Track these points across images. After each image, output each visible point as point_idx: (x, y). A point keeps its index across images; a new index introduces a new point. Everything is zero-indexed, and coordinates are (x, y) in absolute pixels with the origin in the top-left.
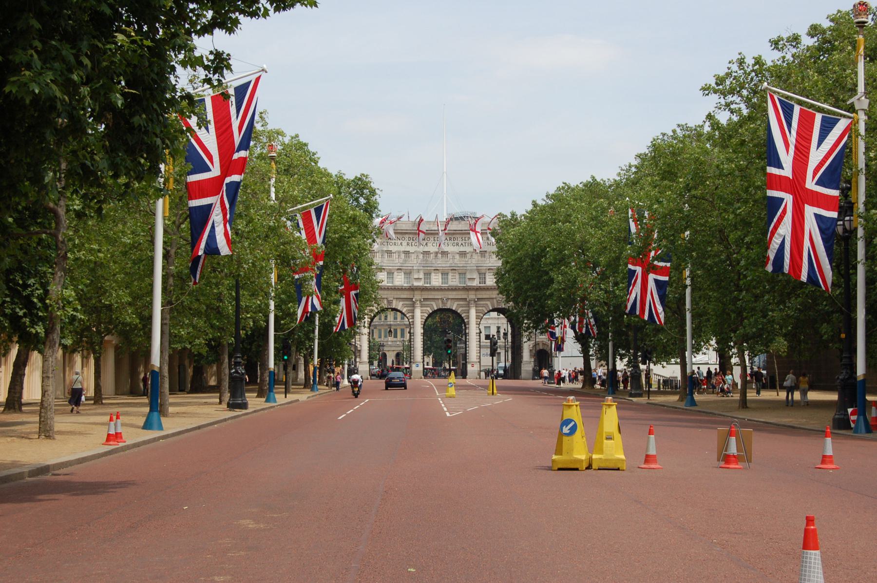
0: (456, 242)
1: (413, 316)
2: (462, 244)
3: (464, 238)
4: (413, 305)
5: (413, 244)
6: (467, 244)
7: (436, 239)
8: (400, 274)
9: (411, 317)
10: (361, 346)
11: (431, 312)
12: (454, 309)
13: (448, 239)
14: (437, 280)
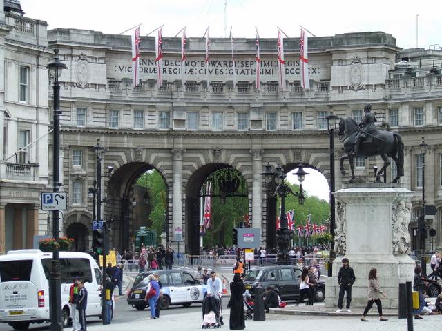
2: (243, 72)
4: (172, 160)
5: (172, 70)
6: (250, 72)
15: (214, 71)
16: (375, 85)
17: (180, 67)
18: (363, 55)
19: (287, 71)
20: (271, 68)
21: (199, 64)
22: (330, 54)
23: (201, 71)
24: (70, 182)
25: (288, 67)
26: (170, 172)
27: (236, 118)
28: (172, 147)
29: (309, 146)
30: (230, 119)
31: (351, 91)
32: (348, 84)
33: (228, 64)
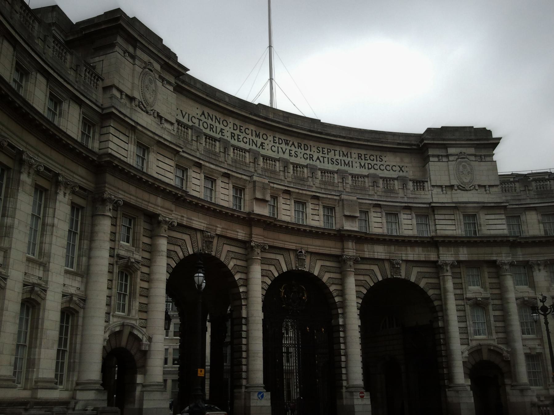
0: (308, 152)
2: (318, 158)
3: (321, 149)
4: (248, 260)
5: (241, 138)
6: (326, 160)
7: (277, 139)
8: (227, 186)
10: (150, 339)
11: (276, 275)
12: (316, 273)
13: (296, 145)
14: (288, 213)
15: (288, 151)
16: (490, 186)
17: (249, 136)
18: (472, 151)
19: (370, 166)
20: (349, 159)
21: (271, 138)
22: (427, 147)
23: (273, 148)
24: (116, 270)
25: (369, 161)
27: (321, 212)
28: (247, 239)
29: (411, 258)
30: (315, 212)
31: (459, 191)
32: (454, 182)
33: (302, 147)
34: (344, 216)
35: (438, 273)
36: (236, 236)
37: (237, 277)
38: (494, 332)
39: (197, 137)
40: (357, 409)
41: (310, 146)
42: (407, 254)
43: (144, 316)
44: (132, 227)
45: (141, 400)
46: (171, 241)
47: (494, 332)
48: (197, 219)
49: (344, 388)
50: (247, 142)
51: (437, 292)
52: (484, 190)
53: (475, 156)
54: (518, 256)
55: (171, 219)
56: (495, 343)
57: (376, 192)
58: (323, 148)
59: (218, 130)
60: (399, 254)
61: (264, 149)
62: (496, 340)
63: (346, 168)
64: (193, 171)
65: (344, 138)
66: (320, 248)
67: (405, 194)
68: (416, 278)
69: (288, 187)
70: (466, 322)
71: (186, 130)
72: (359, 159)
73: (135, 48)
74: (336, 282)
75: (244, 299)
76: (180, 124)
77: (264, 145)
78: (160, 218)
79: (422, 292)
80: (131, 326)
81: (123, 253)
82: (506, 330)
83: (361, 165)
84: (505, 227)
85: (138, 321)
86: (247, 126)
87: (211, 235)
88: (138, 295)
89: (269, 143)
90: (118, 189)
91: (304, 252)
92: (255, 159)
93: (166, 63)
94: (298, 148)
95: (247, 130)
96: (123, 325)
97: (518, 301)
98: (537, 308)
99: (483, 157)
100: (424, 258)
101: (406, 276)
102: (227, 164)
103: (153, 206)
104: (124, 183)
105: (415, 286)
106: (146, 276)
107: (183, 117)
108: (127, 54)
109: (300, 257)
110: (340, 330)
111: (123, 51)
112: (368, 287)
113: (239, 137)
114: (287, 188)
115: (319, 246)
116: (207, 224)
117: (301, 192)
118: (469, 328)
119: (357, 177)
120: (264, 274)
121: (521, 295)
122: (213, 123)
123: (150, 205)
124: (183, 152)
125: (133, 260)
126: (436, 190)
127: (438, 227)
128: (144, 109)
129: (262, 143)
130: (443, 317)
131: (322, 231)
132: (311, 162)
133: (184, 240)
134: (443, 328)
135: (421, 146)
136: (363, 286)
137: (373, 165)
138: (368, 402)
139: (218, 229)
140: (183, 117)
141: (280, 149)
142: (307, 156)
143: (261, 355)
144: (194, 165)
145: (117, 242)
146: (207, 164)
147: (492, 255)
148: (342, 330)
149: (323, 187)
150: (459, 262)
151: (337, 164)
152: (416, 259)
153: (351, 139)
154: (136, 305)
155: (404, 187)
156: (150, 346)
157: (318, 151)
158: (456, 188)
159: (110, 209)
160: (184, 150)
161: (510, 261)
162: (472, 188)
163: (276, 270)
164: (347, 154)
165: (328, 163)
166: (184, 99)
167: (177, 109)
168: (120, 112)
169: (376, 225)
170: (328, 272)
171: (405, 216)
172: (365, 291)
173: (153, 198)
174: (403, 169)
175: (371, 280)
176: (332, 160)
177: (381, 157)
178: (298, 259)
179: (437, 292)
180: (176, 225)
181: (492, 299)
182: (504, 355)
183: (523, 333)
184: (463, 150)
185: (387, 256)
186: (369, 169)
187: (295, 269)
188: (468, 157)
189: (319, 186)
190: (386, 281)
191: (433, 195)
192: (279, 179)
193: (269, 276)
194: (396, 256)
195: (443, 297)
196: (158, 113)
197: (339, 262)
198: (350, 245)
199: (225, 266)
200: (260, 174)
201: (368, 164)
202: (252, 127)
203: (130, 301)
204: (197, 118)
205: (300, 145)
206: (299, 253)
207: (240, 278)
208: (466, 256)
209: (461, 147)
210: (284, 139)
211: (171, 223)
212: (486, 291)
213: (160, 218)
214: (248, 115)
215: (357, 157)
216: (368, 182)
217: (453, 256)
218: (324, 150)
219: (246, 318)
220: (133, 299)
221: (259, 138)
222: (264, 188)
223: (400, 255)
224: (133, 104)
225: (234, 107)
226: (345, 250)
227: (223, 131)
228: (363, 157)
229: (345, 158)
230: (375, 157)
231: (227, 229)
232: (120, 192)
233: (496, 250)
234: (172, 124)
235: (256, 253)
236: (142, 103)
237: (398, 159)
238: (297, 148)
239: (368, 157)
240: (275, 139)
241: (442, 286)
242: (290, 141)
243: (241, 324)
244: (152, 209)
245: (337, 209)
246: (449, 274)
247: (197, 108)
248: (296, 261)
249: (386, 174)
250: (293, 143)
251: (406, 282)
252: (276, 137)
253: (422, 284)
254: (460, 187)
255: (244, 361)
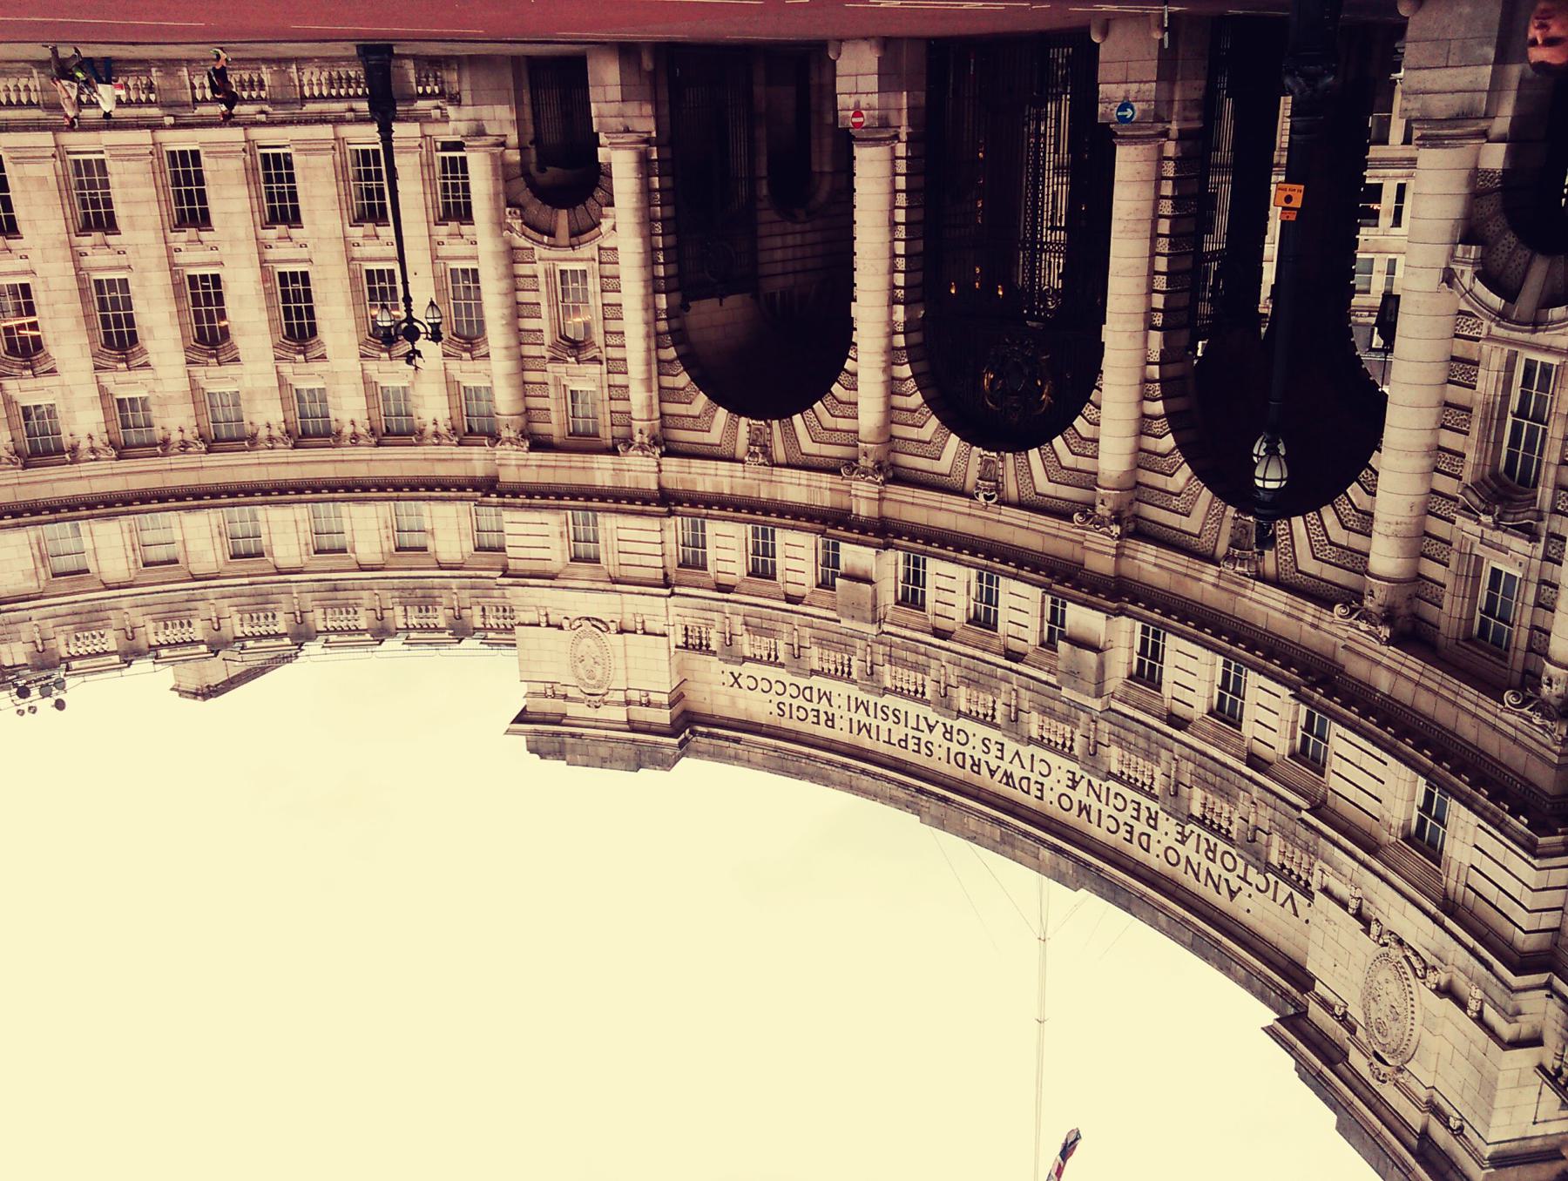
0: (955, 748)
1: (1142, 432)
2: (931, 728)
3: (924, 749)
4: (1134, 488)
5: (1130, 811)
6: (911, 722)
7: (1034, 788)
9: (1158, 426)
10: (1449, 277)
11: (1058, 442)
12: (954, 440)
14: (1015, 601)
15: (1008, 757)
16: (538, 625)
17: (1106, 811)
18: (573, 710)
19: (807, 692)
20: (855, 718)
25: (808, 706)
26: (1150, 443)
28: (1131, 543)
33: (969, 762)
34: (873, 583)
35: (663, 426)
36: (1160, 555)
37: (1169, 442)
38: (542, 279)
39: (1254, 840)
40: (872, 82)
41: (948, 762)
42: (732, 477)
43: (1460, 347)
44: (1478, 615)
45: (1496, 86)
46: (1358, 561)
47: (542, 279)
48: (1271, 612)
49: (904, 137)
50: (1116, 798)
51: (668, 381)
52: (550, 616)
53: (565, 697)
54: (482, 457)
55: (1350, 625)
56: (539, 251)
57: (796, 633)
58: (919, 752)
59: (1192, 841)
60: (750, 478)
61: (1069, 771)
62: (536, 258)
63: (863, 697)
64: (1273, 748)
65: (863, 772)
66: (938, 505)
67: (727, 621)
68: (713, 417)
69: (1011, 670)
70: (604, 305)
71: (1287, 864)
72: (833, 715)
73: (1425, 1134)
74: (905, 416)
75: (1154, 381)
76: (1302, 883)
77: (1070, 783)
78: (1385, 632)
79: (702, 381)
80: (1510, 321)
81: (1519, 545)
82: (514, 283)
83: (829, 700)
84: (508, 528)
85: (1485, 331)
86: (1112, 840)
87: (1235, 565)
88: (1478, 412)
89: (1056, 784)
90: (1515, 740)
91: (981, 496)
92: (1095, 753)
93: (1330, 1063)
94: (979, 760)
95: (1113, 828)
96: (1537, 324)
97: (483, 351)
98: (430, 336)
99: (549, 692)
100: (693, 465)
101: (737, 423)
102: (1172, 751)
103: (1405, 671)
104: (1496, 755)
105: (718, 398)
106: (1443, 467)
107: (1291, 895)
108: (1454, 1124)
109: (993, 484)
110: (903, 292)
111: (1465, 1137)
112: (828, 399)
113: (1135, 814)
114: (1014, 666)
115: (940, 509)
116: (1244, 596)
117: (978, 653)
118: (598, 289)
119: (839, 674)
120: (1091, 446)
121: (480, 365)
122: (1206, 863)
123: (1416, 677)
124: (1298, 808)
125: (1483, 518)
126: (658, 629)
127: (657, 537)
128: (1409, 953)
129: (1074, 788)
130: (657, 319)
131: (929, 548)
132: (949, 722)
133: (1315, 558)
134: (656, 291)
135: (688, 731)
136: (841, 402)
137: (801, 695)
138: (843, 101)
139: (1212, 580)
140: (1291, 895)
141: (1027, 764)
142: (959, 737)
143: (1116, 227)
144: (1270, 764)
145: (1534, 577)
146: (1230, 761)
147: (539, 463)
148: (898, 291)
149: (922, 659)
150: (613, 451)
151: (885, 709)
152: (712, 464)
153: (845, 767)
154: (1487, 383)
155: (730, 639)
156: (1452, 256)
157: (929, 745)
158: (613, 627)
159: (1550, 684)
160: (1295, 813)
161: (498, 446)
162: (577, 623)
163: (1060, 455)
164: (860, 730)
165: (906, 713)
166: (1287, 946)
167: (1307, 921)
168: (1489, 967)
169: (799, 552)
170: (924, 442)
171: (730, 567)
172: (836, 389)
173: (1405, 692)
174: (733, 680)
175: (821, 418)
176: (896, 720)
177: (781, 713)
178: (997, 481)
179: (668, 381)
180: (1337, 606)
181: (544, 357)
182: (520, 221)
183: (475, 271)
184: (591, 713)
185: (778, 473)
186: (811, 688)
187: (1007, 454)
188: (582, 696)
189: (932, 660)
190: (784, 414)
191: (665, 614)
192: (1033, 691)
193: (1078, 439)
194: (758, 473)
195: (654, 367)
196: (1367, 932)
197: (894, 465)
198: (864, 509)
199: (1200, 473)
200: (1084, 712)
201: (811, 701)
202: (1099, 833)
203: (1506, 395)
204: (1251, 884)
205: (976, 768)
206: (993, 496)
207: (1161, 437)
208: (596, 465)
209: (597, 720)
210: (1015, 788)
211: (1350, 615)
212: (556, 377)
213: (1385, 632)
214: (1108, 868)
215: (837, 720)
216: (814, 656)
217: (625, 467)
218: (916, 748)
219: (1150, 326)
220: (1494, 403)
221: (1080, 802)
222: (1074, 674)
223: (747, 475)
224: (1443, 978)
225: (1142, 897)
226: (877, 496)
227: (1179, 837)
228: (823, 718)
229: (865, 720)
230: (794, 717)
231: (1186, 575)
232: (1511, 730)
233: (530, 477)
234: (1326, 891)
235: (1109, 504)
236: (1416, 975)
237: (741, 704)
238: (982, 762)
239: (811, 718)
240: (1039, 794)
241: (655, 394)
242: (1000, 782)
243: (1165, 311)
244: (1408, 663)
245: (890, 600)
246: (637, 425)
247: (1248, 911)
248: (1002, 476)
249: (772, 673)
250: (992, 776)
251: (737, 408)
252: (1036, 797)
253: (702, 398)
254: (604, 629)
255: (1166, 207)
